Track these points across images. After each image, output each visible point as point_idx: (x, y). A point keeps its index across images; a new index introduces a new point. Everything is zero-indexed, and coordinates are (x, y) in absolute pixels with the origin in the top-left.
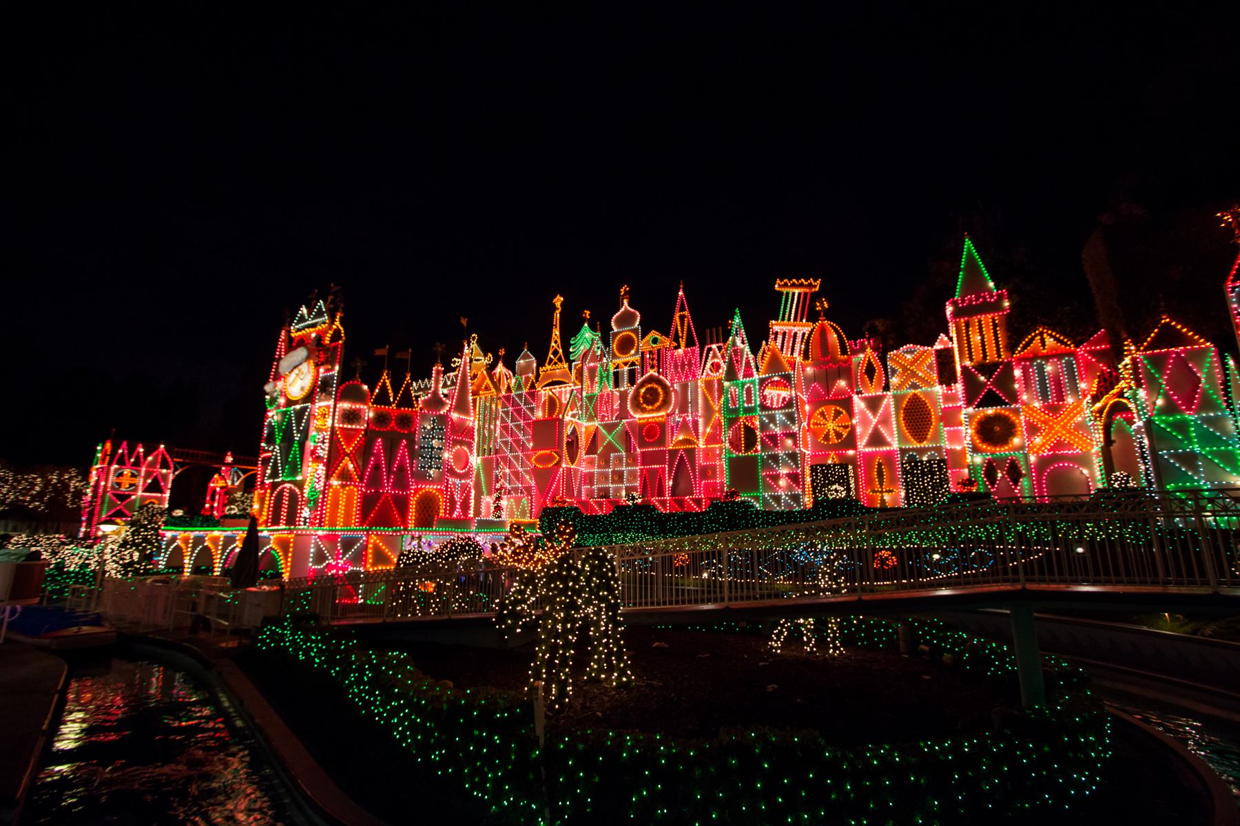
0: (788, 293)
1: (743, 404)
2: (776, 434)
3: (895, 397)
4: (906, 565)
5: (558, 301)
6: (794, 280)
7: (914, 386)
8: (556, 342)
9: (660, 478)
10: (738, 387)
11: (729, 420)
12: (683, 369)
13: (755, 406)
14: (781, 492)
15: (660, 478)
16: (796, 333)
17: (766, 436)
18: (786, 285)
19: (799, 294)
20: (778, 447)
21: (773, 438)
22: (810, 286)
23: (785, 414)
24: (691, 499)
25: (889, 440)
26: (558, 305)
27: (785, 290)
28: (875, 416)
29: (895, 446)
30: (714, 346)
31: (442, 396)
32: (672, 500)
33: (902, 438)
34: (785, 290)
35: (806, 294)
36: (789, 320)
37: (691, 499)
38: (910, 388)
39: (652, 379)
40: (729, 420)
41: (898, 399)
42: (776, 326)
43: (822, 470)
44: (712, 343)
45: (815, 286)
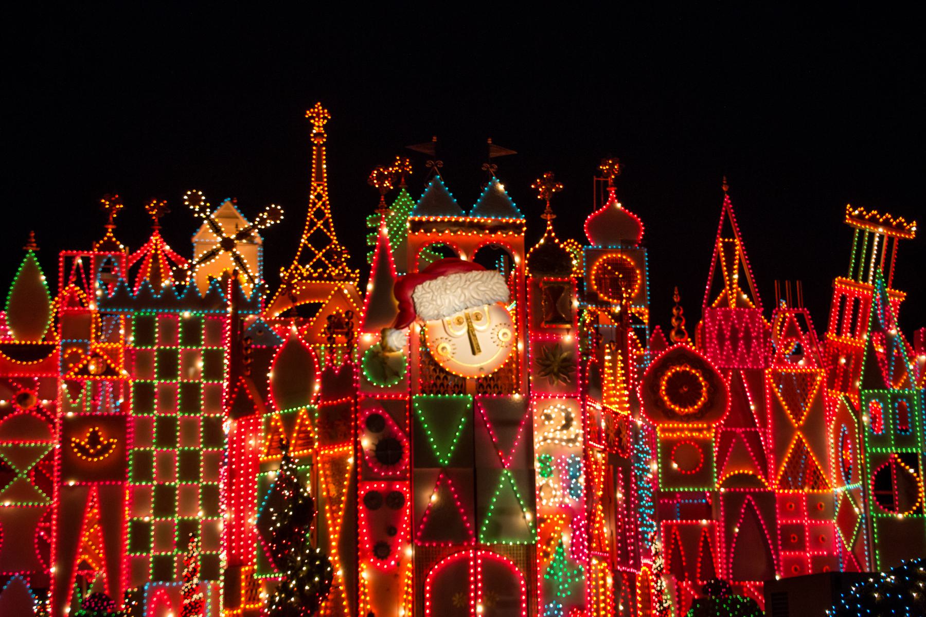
0: (862, 232)
9: (705, 542)
15: (705, 542)
18: (860, 217)
19: (881, 237)
22: (900, 227)
35: (891, 239)
36: (865, 279)
39: (682, 356)
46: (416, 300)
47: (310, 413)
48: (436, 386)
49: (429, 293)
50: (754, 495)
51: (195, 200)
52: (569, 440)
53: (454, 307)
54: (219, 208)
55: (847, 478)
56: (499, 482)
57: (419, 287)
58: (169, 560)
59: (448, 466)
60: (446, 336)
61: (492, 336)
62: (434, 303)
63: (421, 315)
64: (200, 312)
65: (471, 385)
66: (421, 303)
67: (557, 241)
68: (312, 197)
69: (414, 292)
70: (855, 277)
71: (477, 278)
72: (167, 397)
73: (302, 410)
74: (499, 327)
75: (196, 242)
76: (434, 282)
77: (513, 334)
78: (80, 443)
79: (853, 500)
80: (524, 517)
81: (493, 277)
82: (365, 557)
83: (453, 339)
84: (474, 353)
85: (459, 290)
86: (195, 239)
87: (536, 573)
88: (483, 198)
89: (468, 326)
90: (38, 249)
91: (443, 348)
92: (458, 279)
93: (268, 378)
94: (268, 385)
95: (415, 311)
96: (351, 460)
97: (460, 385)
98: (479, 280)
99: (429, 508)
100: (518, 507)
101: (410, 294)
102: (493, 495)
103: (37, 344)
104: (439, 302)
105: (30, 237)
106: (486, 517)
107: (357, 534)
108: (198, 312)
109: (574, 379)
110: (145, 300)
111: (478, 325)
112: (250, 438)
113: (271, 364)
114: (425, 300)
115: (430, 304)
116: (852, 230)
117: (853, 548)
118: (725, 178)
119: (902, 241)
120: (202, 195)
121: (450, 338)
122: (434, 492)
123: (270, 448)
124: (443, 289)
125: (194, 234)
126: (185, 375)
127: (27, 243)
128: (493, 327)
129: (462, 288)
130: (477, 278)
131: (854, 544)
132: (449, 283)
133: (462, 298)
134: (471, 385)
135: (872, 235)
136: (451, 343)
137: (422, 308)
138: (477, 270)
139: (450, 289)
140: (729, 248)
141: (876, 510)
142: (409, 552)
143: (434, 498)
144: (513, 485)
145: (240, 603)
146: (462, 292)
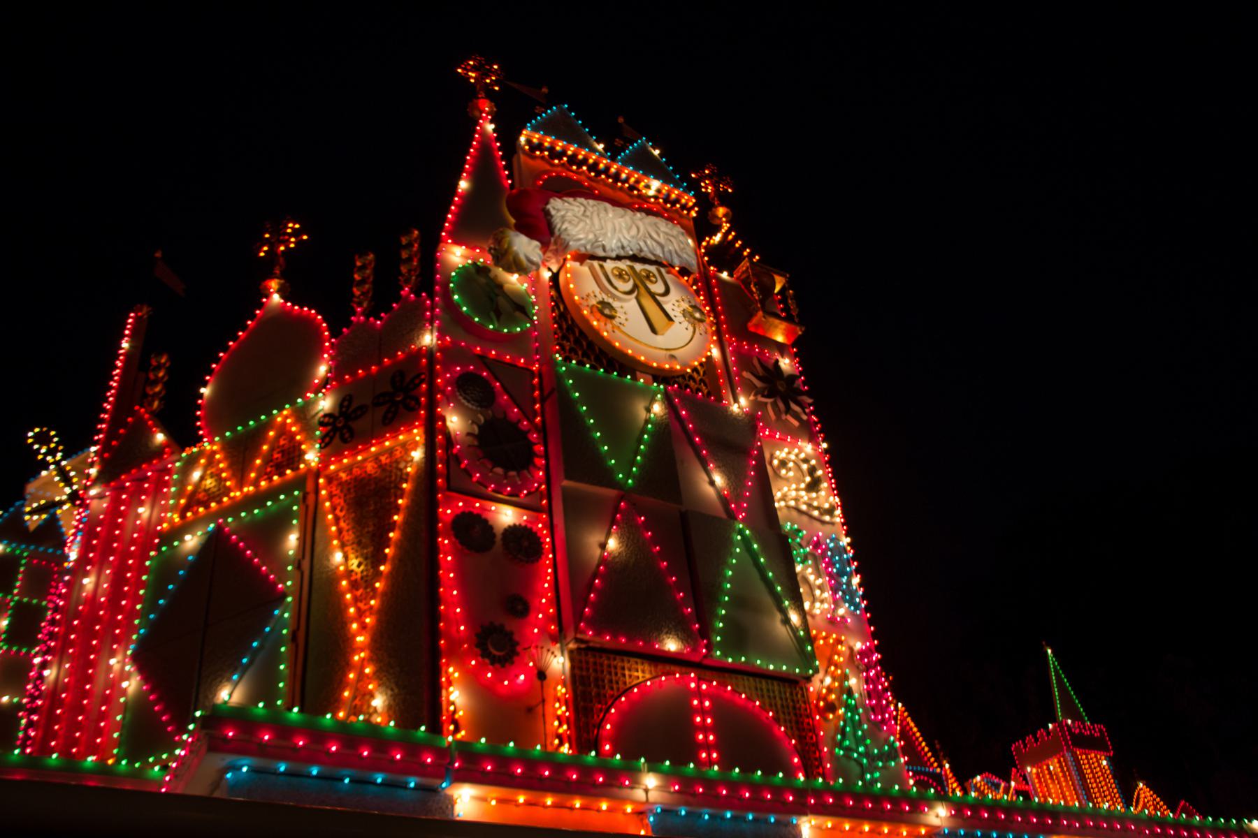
46: (553, 212)
51: (43, 439)
54: (61, 523)
56: (729, 543)
59: (632, 489)
64: (23, 547)
75: (30, 494)
80: (787, 621)
86: (31, 488)
87: (817, 746)
93: (201, 396)
94: (199, 407)
96: (418, 455)
99: (603, 560)
100: (768, 600)
102: (722, 563)
106: (717, 602)
108: (18, 546)
112: (141, 504)
113: (210, 372)
120: (54, 436)
122: (608, 535)
125: (32, 479)
142: (558, 663)
143: (613, 544)
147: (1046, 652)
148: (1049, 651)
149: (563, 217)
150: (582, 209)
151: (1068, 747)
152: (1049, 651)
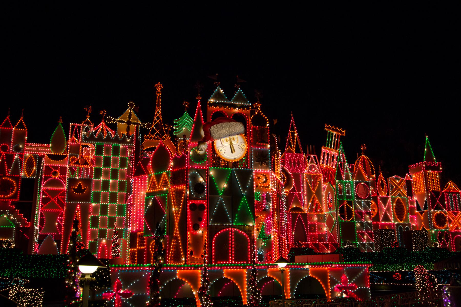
0: (330, 133)
1: (346, 194)
2: (362, 212)
3: (392, 198)
4: (84, 284)
5: (159, 87)
6: (333, 127)
7: (399, 195)
8: (158, 118)
10: (342, 184)
11: (340, 201)
12: (294, 165)
13: (352, 195)
14: (365, 242)
16: (334, 155)
17: (357, 212)
18: (329, 128)
19: (335, 135)
20: (363, 219)
21: (361, 213)
22: (340, 132)
23: (365, 202)
24: (323, 244)
25: (391, 219)
26: (159, 89)
27: (329, 131)
28: (385, 207)
29: (393, 222)
30: (312, 156)
31: (89, 145)
32: (313, 244)
33: (395, 220)
34: (329, 131)
35: (338, 136)
36: (331, 147)
37: (323, 244)
38: (398, 196)
40: (340, 201)
41: (393, 200)
42: (324, 150)
43: (385, 232)
44: (310, 154)
45: (343, 133)
46: (211, 131)
47: (168, 174)
48: (217, 164)
49: (216, 129)
50: (301, 214)
52: (266, 187)
53: (225, 135)
55: (330, 209)
57: (213, 126)
58: (105, 231)
60: (222, 146)
61: (239, 146)
62: (218, 132)
63: (213, 137)
65: (230, 165)
66: (213, 132)
67: (262, 114)
68: (156, 112)
69: (210, 128)
70: (328, 146)
71: (234, 124)
72: (106, 173)
73: (164, 173)
74: (242, 143)
76: (218, 125)
77: (246, 147)
78: (74, 188)
79: (332, 216)
81: (240, 124)
82: (190, 230)
83: (225, 147)
84: (232, 153)
85: (228, 129)
88: (236, 96)
89: (230, 142)
90: (63, 122)
91: (221, 150)
92: (227, 124)
95: (211, 135)
97: (227, 164)
98: (235, 125)
101: (209, 129)
103: (61, 155)
104: (220, 132)
105: (60, 118)
107: (186, 221)
109: (267, 164)
110: (100, 139)
111: (234, 142)
114: (215, 131)
115: (217, 133)
116: (327, 132)
117: (332, 231)
118: (292, 112)
119: (342, 137)
121: (223, 147)
123: (150, 187)
124: (222, 128)
126: (113, 166)
127: (59, 120)
128: (239, 143)
129: (229, 128)
130: (234, 124)
131: (332, 230)
132: (224, 126)
133: (229, 132)
134: (230, 165)
135: (333, 134)
136: (224, 148)
137: (214, 134)
138: (234, 121)
139: (224, 128)
140: (293, 134)
141: (340, 219)
144: (246, 204)
145: (136, 246)
146: (229, 129)
147: (426, 137)
148: (427, 137)
149: (213, 132)
150: (217, 129)
151: (423, 169)
152: (427, 137)
